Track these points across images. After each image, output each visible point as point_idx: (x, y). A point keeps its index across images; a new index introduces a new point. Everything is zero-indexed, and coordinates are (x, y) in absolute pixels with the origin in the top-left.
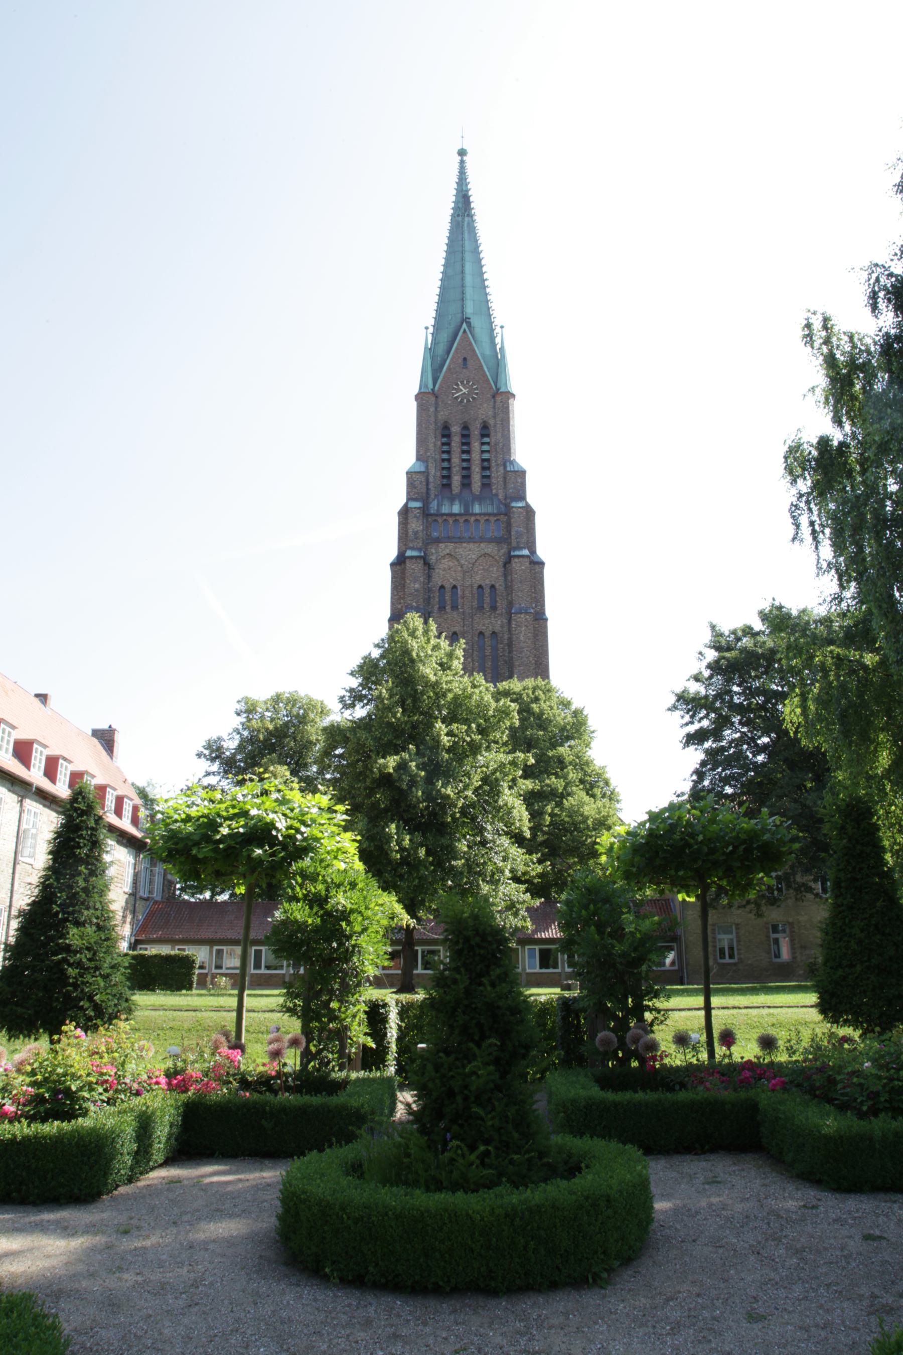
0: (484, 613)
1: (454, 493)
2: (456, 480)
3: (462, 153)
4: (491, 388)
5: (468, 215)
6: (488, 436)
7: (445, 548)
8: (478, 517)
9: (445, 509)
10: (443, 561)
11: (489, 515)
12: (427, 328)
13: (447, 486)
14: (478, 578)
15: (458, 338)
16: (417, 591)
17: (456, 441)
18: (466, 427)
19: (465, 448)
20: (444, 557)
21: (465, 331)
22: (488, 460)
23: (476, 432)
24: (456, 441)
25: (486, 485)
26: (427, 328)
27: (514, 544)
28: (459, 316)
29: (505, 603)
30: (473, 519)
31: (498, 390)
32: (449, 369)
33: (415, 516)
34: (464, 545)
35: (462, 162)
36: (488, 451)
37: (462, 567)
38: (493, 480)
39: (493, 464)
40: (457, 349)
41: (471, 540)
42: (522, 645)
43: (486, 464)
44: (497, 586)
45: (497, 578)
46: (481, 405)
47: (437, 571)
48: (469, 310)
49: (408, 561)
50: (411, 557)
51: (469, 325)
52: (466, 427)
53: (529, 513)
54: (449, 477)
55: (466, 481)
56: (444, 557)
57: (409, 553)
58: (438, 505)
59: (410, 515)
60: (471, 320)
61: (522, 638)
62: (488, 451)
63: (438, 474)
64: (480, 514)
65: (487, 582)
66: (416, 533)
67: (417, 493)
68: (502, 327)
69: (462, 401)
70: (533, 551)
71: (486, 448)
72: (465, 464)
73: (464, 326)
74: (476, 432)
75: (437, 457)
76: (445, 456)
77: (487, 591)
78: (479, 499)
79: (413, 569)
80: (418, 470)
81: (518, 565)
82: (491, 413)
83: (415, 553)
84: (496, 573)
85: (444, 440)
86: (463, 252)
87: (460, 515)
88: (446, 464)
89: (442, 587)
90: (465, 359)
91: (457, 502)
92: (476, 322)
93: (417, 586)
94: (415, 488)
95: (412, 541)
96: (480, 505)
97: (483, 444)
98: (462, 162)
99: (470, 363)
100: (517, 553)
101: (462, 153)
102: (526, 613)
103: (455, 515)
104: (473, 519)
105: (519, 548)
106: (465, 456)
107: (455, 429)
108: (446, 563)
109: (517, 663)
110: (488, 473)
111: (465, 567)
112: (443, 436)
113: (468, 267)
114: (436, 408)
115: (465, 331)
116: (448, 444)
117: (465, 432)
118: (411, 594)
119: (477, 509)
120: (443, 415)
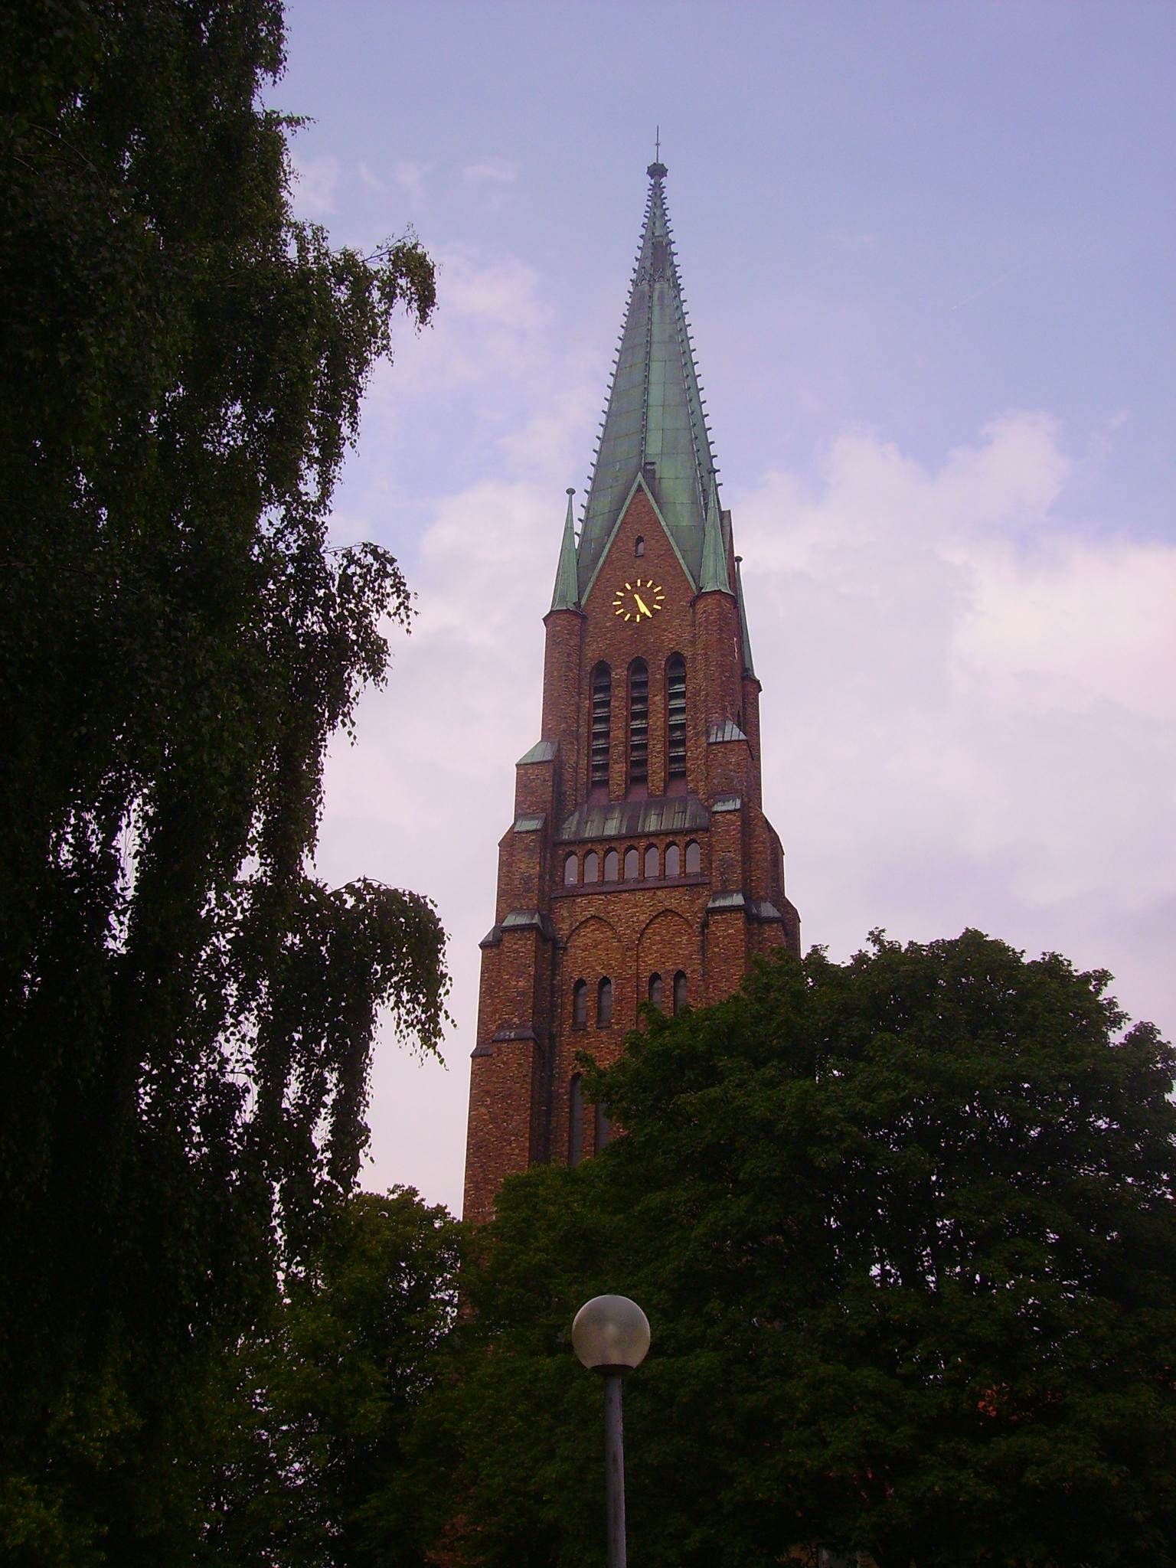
2: (618, 770)
3: (657, 171)
4: (689, 588)
6: (682, 680)
7: (586, 908)
9: (590, 831)
11: (675, 833)
12: (571, 492)
16: (522, 994)
17: (620, 692)
18: (639, 665)
21: (640, 486)
23: (657, 673)
24: (620, 692)
25: (676, 776)
26: (571, 492)
30: (643, 843)
33: (526, 849)
36: (681, 710)
41: (642, 885)
45: (689, 957)
46: (668, 622)
48: (653, 448)
52: (639, 665)
55: (637, 772)
58: (579, 823)
60: (655, 467)
62: (681, 710)
63: (583, 762)
65: (669, 966)
74: (657, 673)
75: (583, 730)
78: (659, 803)
79: (517, 951)
80: (540, 759)
83: (522, 920)
84: (686, 944)
85: (599, 697)
86: (649, 343)
87: (619, 838)
88: (600, 743)
89: (581, 983)
94: (532, 793)
96: (659, 815)
100: (721, 903)
101: (657, 171)
103: (610, 839)
104: (643, 843)
105: (726, 893)
107: (619, 674)
110: (681, 751)
112: (598, 690)
114: (582, 638)
115: (640, 489)
116: (606, 704)
117: (638, 678)
119: (653, 824)
120: (594, 651)
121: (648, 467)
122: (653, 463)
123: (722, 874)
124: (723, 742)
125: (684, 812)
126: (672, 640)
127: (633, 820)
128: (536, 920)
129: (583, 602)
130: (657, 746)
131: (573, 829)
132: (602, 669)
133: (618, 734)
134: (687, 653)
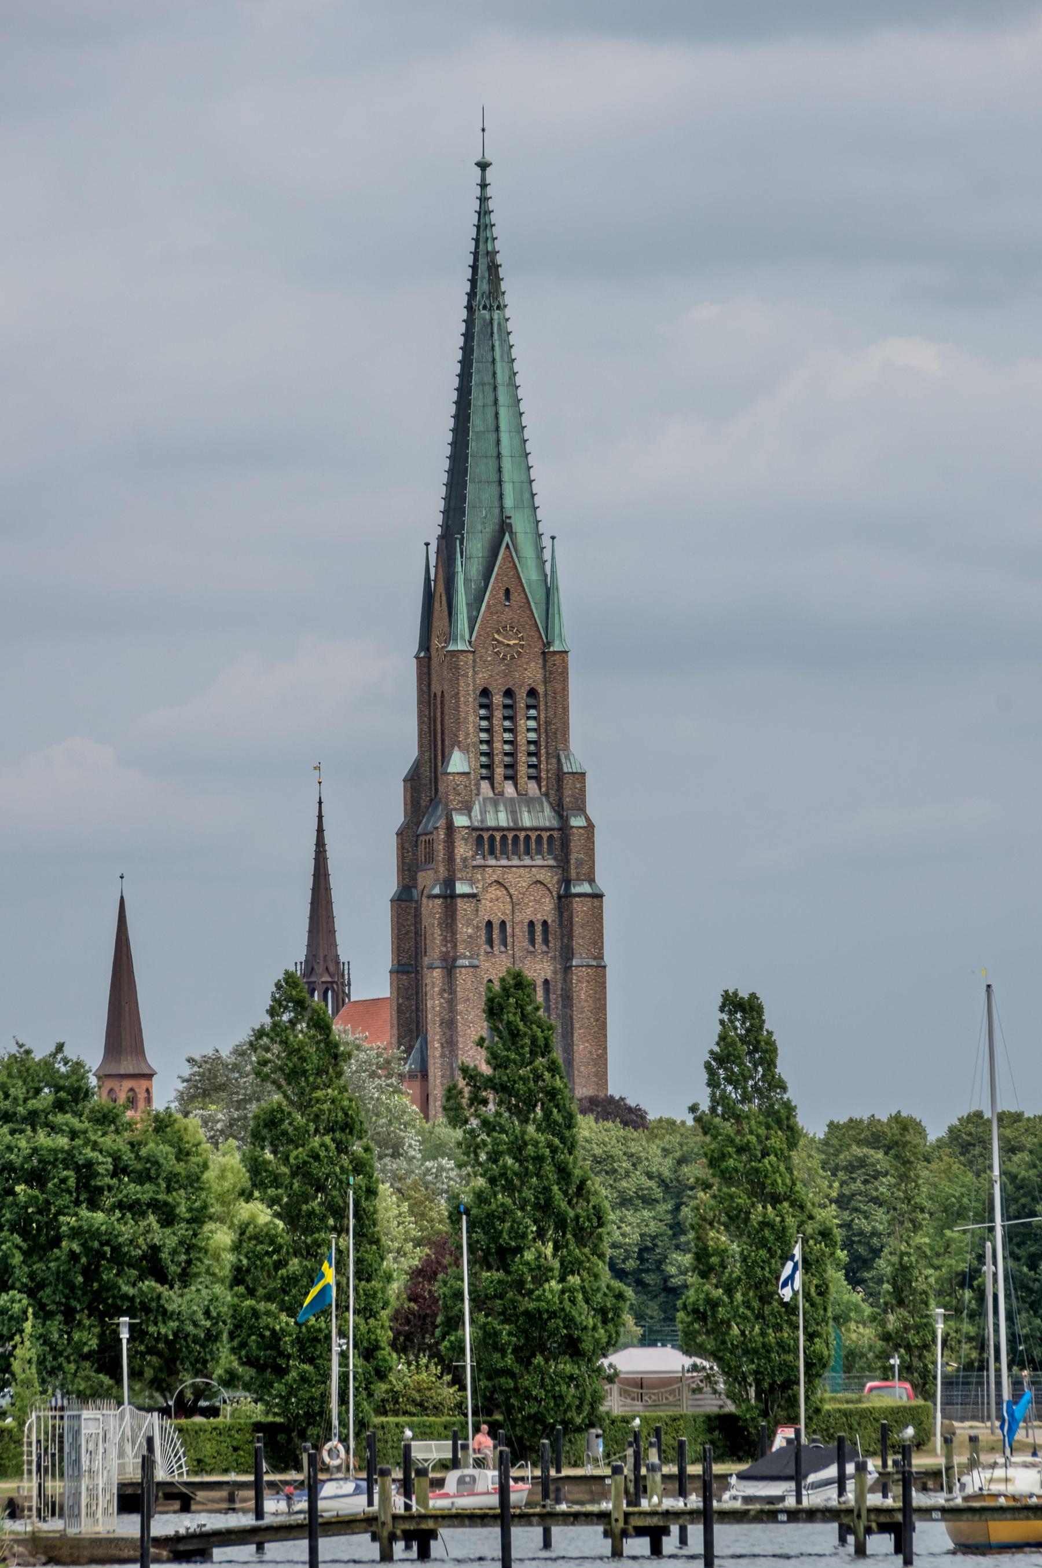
0: (535, 956)
1: (496, 791)
3: (483, 166)
5: (498, 308)
6: (534, 707)
8: (529, 833)
9: (491, 823)
10: (490, 890)
13: (490, 779)
14: (529, 911)
15: (500, 558)
16: (470, 937)
17: (498, 714)
18: (509, 693)
19: (507, 723)
20: (490, 885)
21: (507, 545)
22: (534, 742)
27: (573, 875)
28: (497, 511)
29: (559, 944)
31: (549, 644)
32: (488, 606)
33: (463, 839)
34: (514, 869)
35: (483, 186)
37: (511, 897)
38: (543, 775)
39: (543, 751)
40: (497, 575)
42: (583, 1004)
43: (532, 748)
44: (549, 921)
46: (527, 663)
47: (483, 901)
48: (509, 502)
49: (459, 901)
50: (463, 896)
51: (510, 525)
52: (509, 693)
53: (590, 827)
54: (488, 767)
55: (510, 772)
56: (490, 885)
57: (461, 888)
59: (458, 837)
60: (512, 521)
61: (583, 997)
64: (531, 829)
65: (539, 916)
66: (465, 860)
67: (459, 802)
68: (553, 538)
69: (504, 659)
70: (591, 881)
71: (532, 724)
72: (507, 748)
73: (507, 538)
76: (484, 736)
77: (539, 928)
79: (465, 910)
80: (461, 770)
81: (580, 905)
82: (540, 676)
88: (484, 747)
90: (507, 591)
91: (502, 808)
92: (520, 524)
93: (470, 931)
94: (459, 794)
95: (461, 870)
96: (529, 811)
97: (528, 718)
98: (483, 186)
99: (515, 596)
101: (483, 166)
102: (588, 966)
104: (522, 835)
106: (507, 736)
107: (498, 699)
108: (495, 892)
109: (577, 1025)
111: (514, 898)
112: (482, 706)
113: (503, 412)
115: (507, 545)
117: (508, 702)
118: (464, 941)
120: (482, 678)
121: (508, 521)
122: (510, 518)
123: (576, 868)
124: (573, 773)
125: (543, 812)
126: (530, 678)
127: (514, 814)
128: (475, 891)
129: (473, 639)
130: (522, 758)
131: (479, 817)
132: (485, 693)
133: (498, 745)
134: (541, 690)
